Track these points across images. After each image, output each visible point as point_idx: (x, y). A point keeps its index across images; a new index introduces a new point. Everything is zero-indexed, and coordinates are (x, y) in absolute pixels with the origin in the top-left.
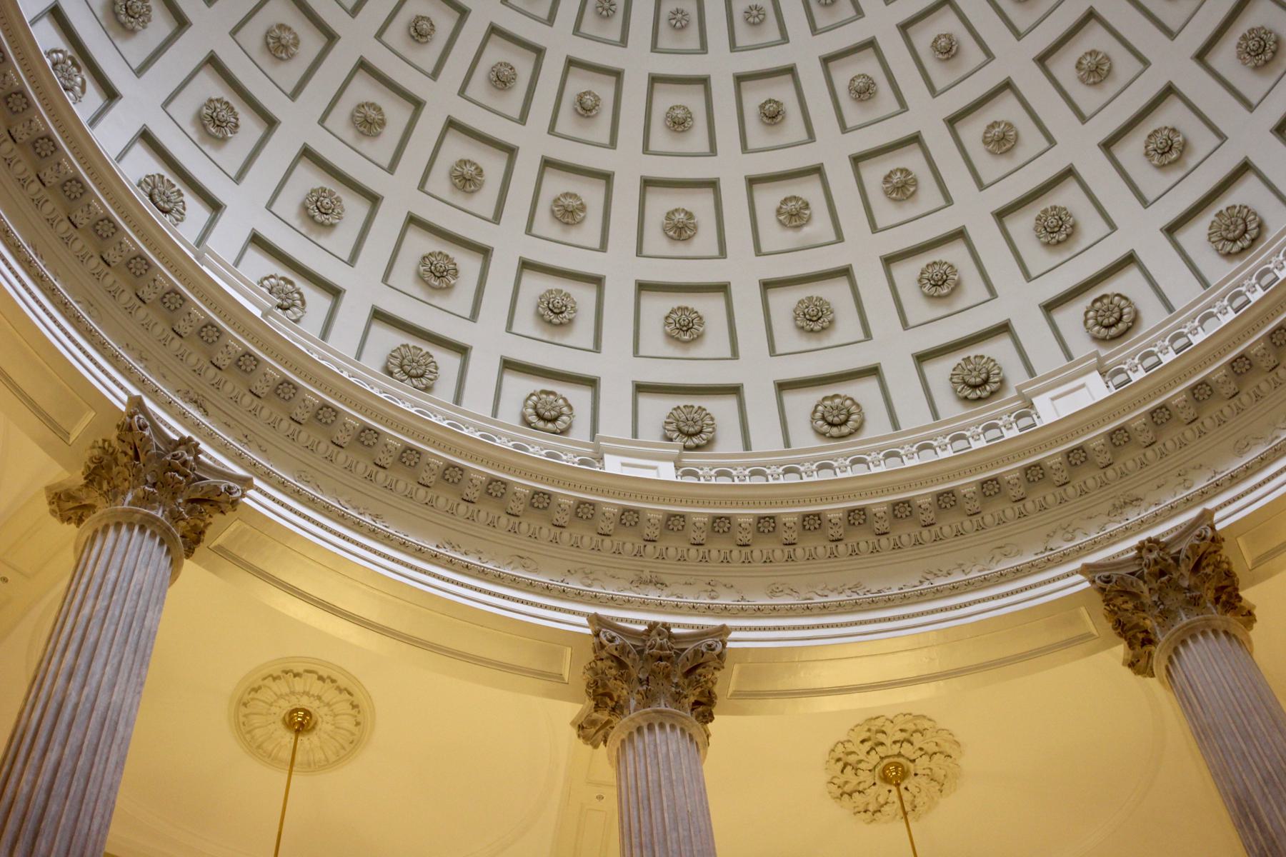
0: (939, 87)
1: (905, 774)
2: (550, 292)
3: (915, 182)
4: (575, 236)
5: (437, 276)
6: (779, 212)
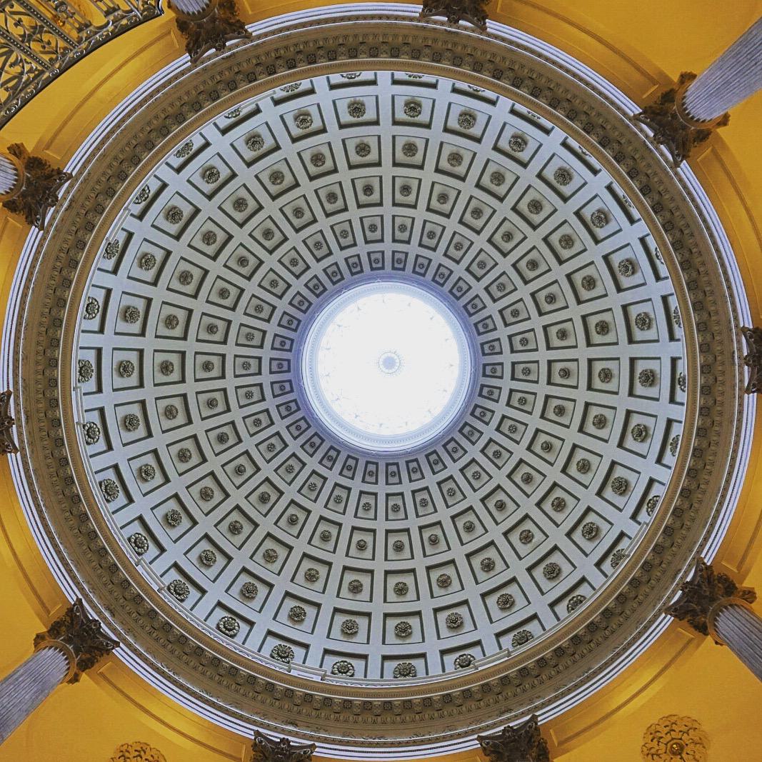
1: (681, 748)
3: (563, 500)
6: (521, 539)
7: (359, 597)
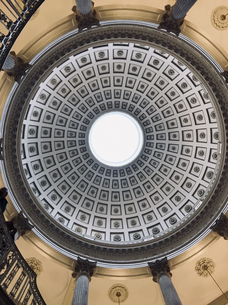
0: (167, 103)
3: (180, 104)
4: (191, 150)
6: (186, 123)
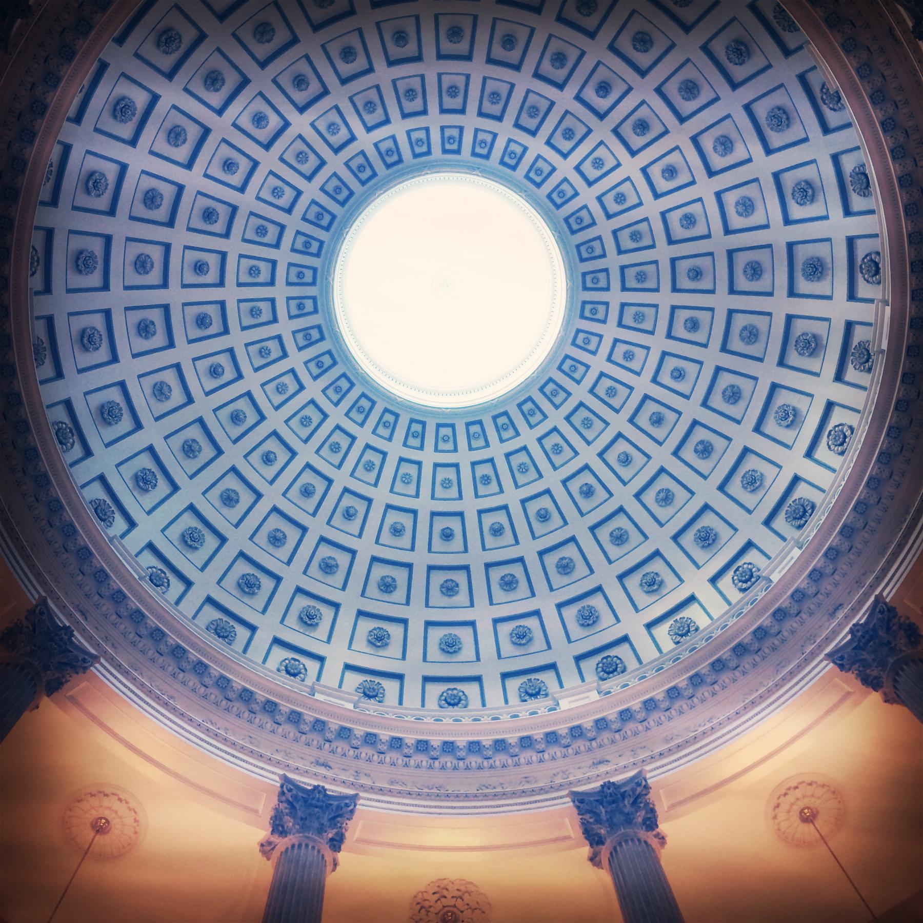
2: (309, 607)
3: (517, 582)
4: (330, 579)
5: (248, 586)
6: (442, 586)
7: (225, 511)
